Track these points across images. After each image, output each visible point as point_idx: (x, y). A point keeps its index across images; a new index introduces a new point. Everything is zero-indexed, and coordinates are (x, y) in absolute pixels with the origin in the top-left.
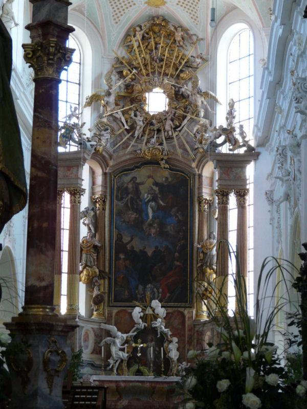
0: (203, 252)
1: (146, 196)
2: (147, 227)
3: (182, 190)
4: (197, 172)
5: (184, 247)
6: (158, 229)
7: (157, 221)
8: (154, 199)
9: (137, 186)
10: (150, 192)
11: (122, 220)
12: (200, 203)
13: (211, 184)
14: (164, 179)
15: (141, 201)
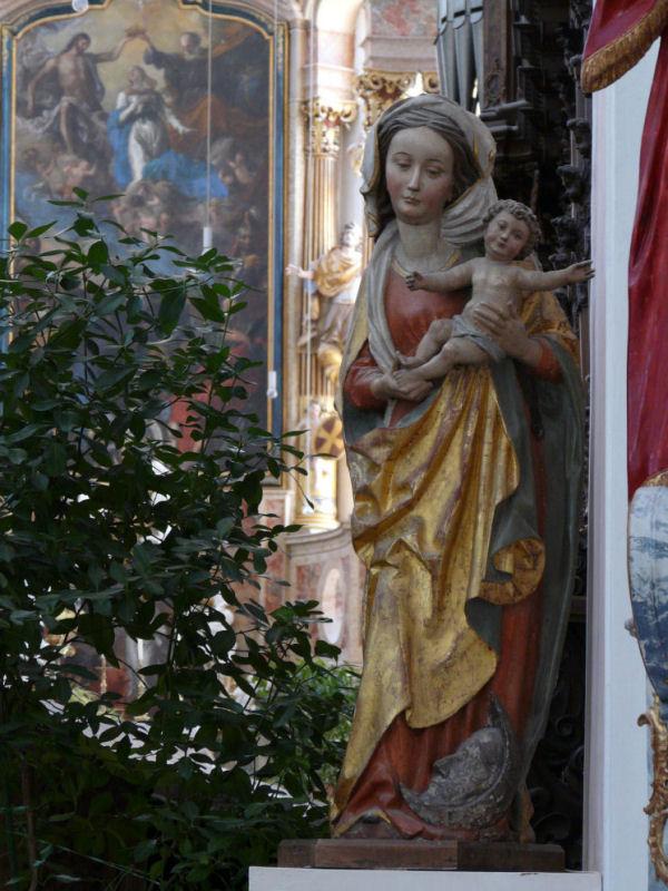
0: (318, 294)
1: (121, 102)
2: (125, 210)
3: (245, 77)
4: (299, 16)
5: (256, 277)
6: (164, 217)
7: (160, 186)
8: (151, 111)
9: (90, 65)
10: (135, 87)
11: (41, 185)
12: (307, 125)
13: (350, 62)
14: (184, 41)
15: (104, 117)
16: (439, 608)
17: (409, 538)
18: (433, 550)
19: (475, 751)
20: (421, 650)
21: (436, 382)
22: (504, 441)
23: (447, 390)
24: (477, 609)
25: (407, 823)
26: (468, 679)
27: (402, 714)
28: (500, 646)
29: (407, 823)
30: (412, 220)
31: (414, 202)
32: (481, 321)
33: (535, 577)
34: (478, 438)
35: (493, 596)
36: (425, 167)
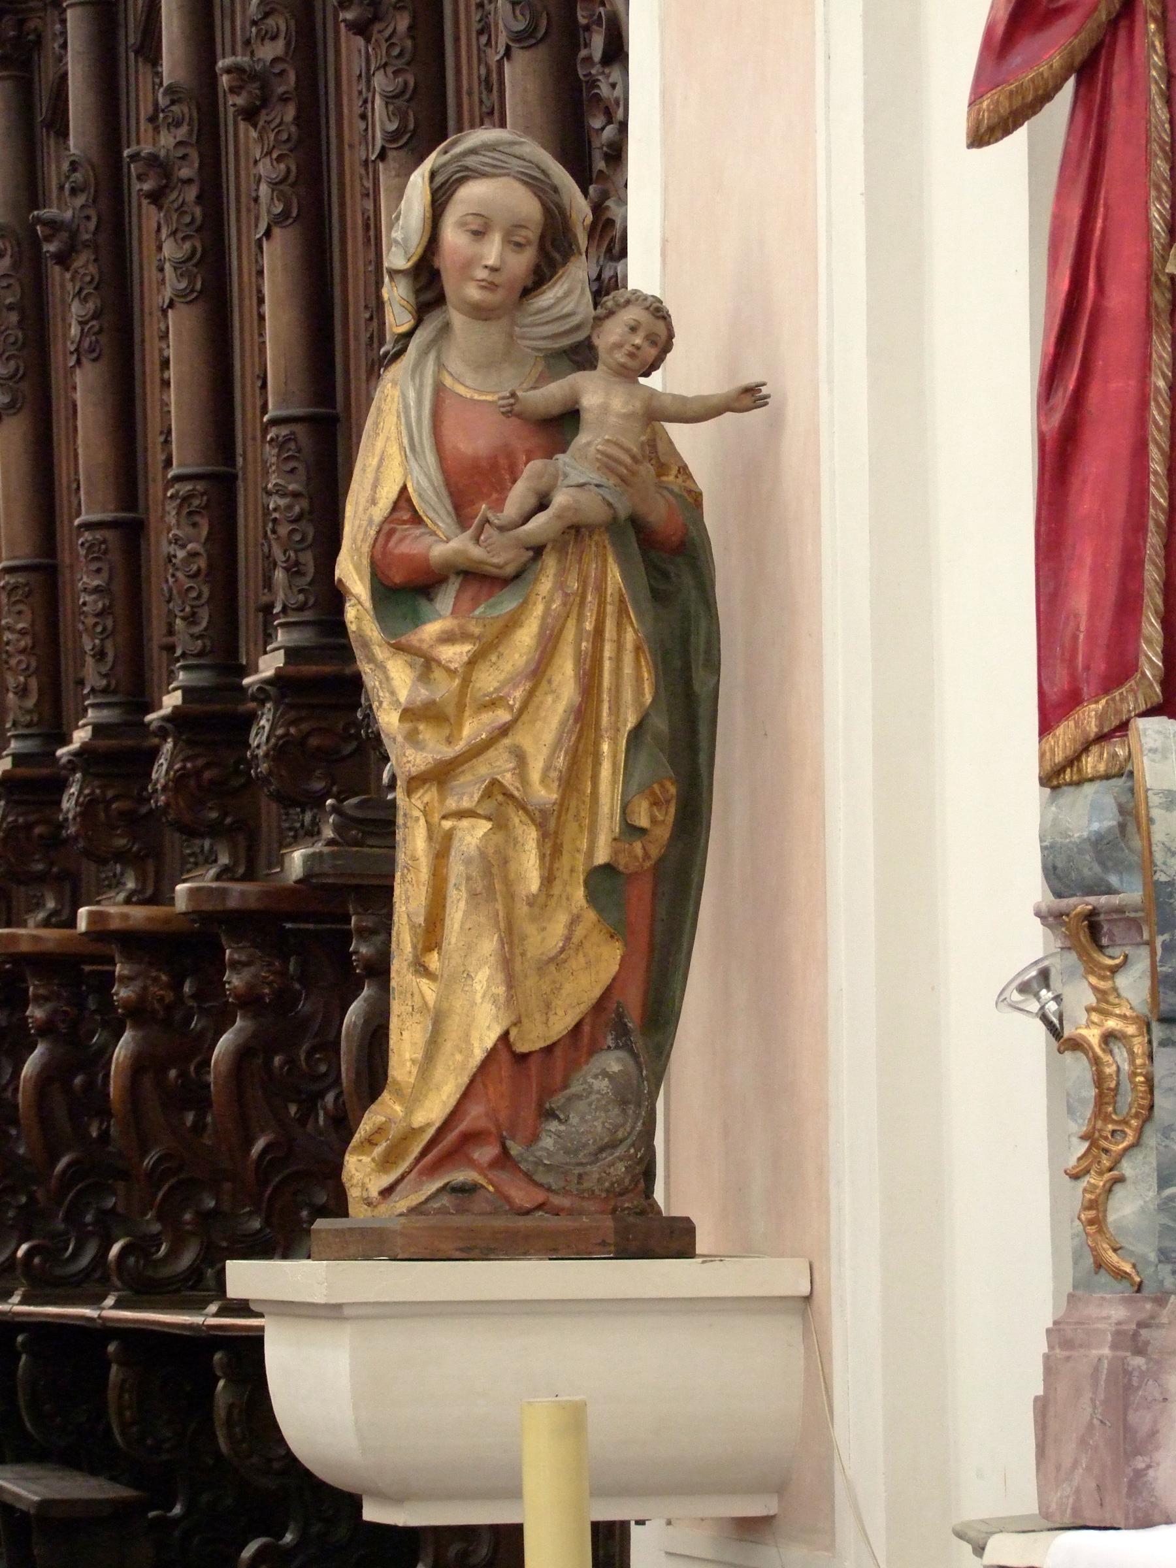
16: (548, 880)
17: (508, 779)
18: (544, 794)
19: (603, 1085)
20: (523, 938)
21: (538, 551)
22: (630, 637)
23: (550, 563)
24: (604, 882)
25: (522, 1195)
26: (585, 980)
27: (505, 1037)
28: (618, 930)
29: (522, 1195)
30: (480, 313)
31: (491, 286)
32: (608, 464)
33: (663, 833)
34: (599, 631)
35: (622, 863)
36: (513, 243)
